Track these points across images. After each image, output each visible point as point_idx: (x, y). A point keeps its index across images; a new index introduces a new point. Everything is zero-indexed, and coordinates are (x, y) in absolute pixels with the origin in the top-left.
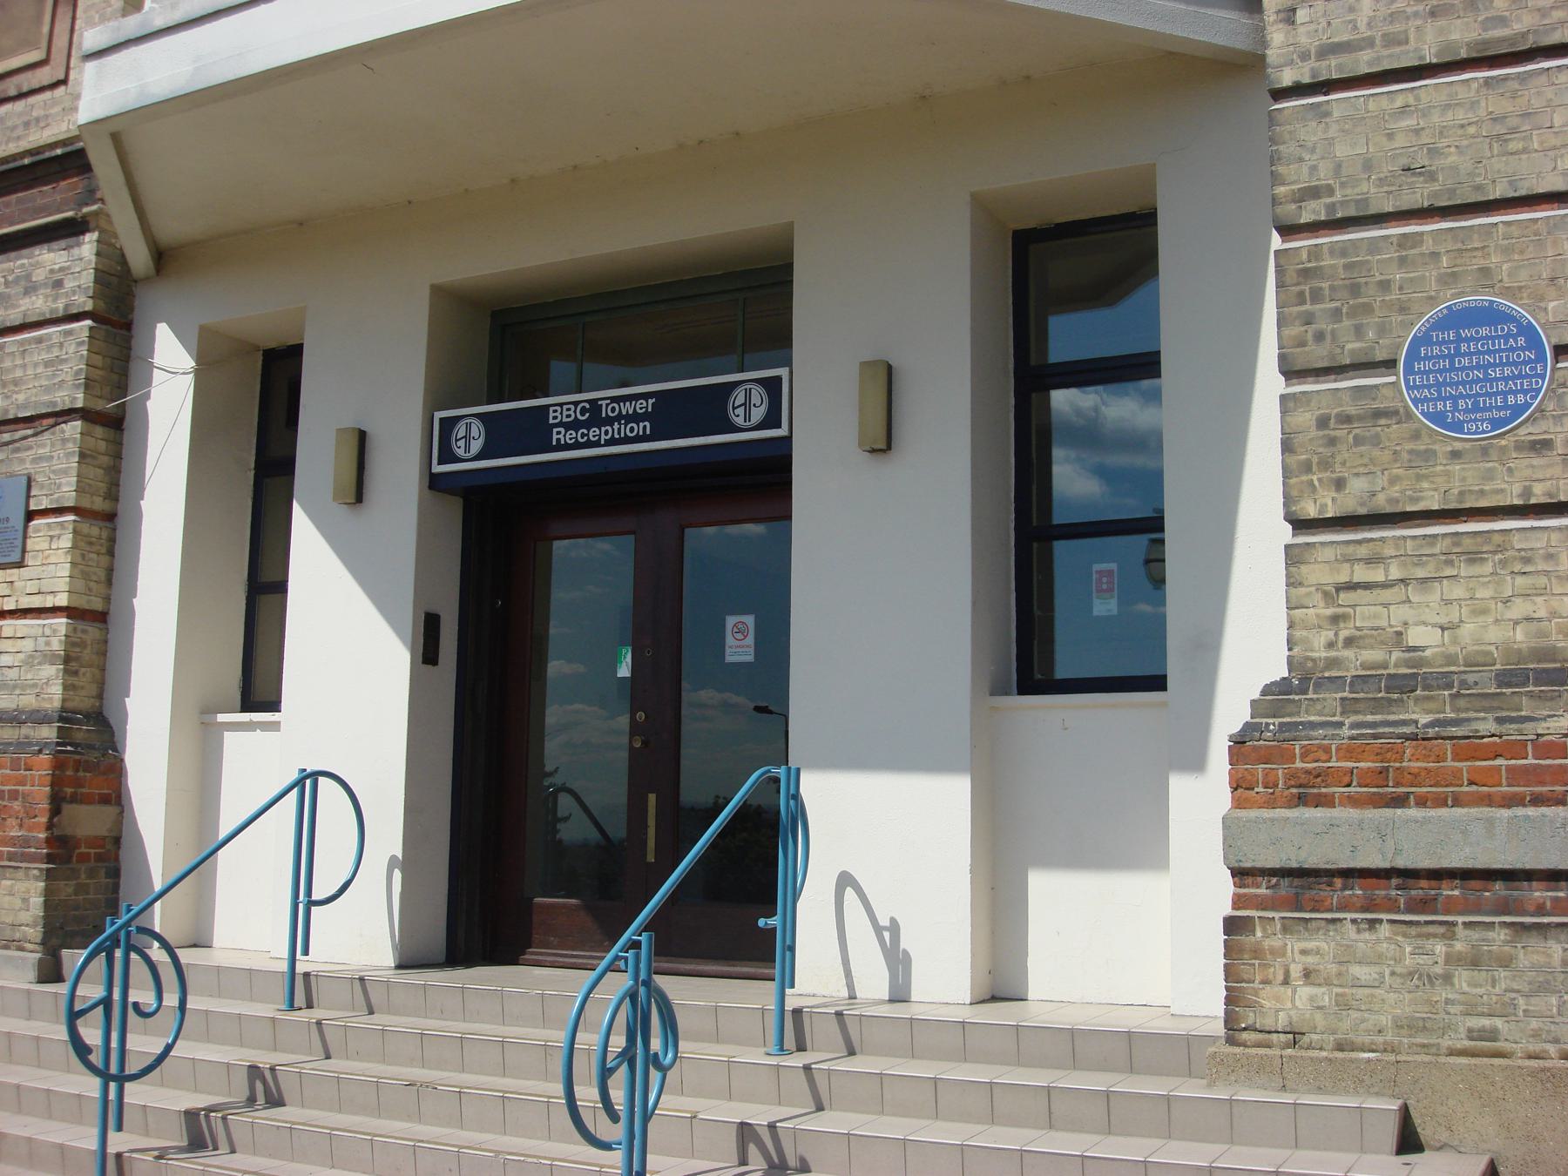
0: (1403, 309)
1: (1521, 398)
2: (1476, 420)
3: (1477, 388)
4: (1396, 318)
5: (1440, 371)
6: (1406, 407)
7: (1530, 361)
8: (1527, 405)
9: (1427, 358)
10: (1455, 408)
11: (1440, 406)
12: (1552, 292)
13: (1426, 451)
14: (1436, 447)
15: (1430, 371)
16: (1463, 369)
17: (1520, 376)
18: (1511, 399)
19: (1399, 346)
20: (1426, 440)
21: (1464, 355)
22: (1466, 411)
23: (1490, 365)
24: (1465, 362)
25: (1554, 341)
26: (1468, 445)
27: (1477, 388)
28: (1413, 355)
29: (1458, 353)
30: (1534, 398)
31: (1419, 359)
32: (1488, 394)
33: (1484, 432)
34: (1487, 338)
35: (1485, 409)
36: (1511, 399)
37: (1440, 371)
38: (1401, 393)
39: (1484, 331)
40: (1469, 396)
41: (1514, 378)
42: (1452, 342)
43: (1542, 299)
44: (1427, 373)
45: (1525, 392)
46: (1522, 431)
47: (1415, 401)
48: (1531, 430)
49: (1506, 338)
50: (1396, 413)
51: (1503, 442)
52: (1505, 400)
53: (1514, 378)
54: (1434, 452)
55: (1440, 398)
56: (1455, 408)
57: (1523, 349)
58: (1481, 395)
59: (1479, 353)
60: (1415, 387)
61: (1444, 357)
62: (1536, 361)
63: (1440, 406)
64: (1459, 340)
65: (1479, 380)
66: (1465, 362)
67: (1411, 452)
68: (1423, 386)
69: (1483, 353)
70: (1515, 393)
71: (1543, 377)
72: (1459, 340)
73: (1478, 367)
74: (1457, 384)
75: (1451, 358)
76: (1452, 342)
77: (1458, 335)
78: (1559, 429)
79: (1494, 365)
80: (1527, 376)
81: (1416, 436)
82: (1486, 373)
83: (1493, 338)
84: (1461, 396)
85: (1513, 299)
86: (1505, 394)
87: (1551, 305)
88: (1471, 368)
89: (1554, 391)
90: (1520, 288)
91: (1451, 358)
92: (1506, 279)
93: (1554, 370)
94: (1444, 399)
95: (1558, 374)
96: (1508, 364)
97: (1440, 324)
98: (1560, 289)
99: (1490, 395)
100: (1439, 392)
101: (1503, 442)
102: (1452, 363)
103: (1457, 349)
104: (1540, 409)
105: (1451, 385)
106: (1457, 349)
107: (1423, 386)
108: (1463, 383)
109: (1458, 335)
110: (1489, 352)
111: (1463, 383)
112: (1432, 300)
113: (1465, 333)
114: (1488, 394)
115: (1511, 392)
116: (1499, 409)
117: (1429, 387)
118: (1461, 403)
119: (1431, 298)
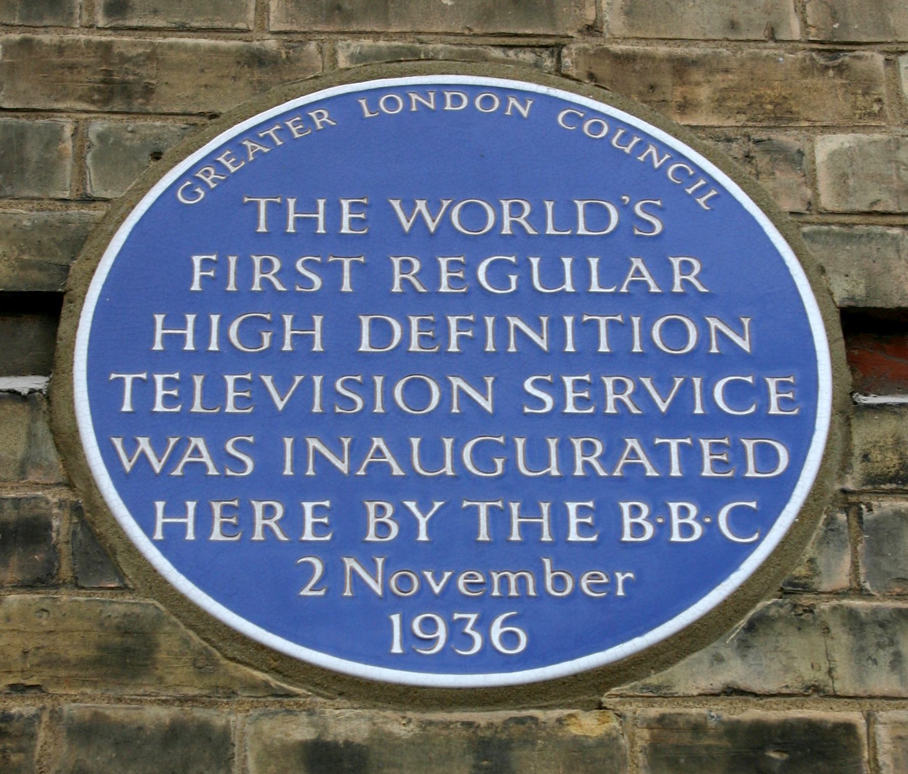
0: (118, 88)
1: (685, 521)
2: (449, 601)
3: (460, 456)
4: (78, 124)
5: (281, 364)
6: (88, 511)
7: (730, 360)
8: (718, 557)
9: (215, 298)
10: (346, 534)
11: (265, 519)
12: (828, 96)
13: (173, 734)
14: (220, 717)
15: (229, 358)
16: (397, 362)
17: (678, 419)
18: (635, 520)
19: (83, 243)
20: (180, 676)
21: (407, 303)
22: (404, 552)
23: (531, 359)
24: (408, 333)
25: (844, 289)
26: (400, 725)
27: (460, 456)
28: (150, 278)
29: (374, 292)
30: (761, 521)
31: (178, 303)
32: (510, 485)
33: (489, 660)
34: (520, 242)
35: (499, 553)
36: (635, 520)
37: (281, 364)
38: (68, 445)
39: (502, 216)
40: (424, 491)
41: (649, 424)
42: (347, 244)
43: (782, 115)
44: (214, 365)
45: (708, 496)
46: (692, 676)
47: (139, 487)
48: (736, 672)
49: (615, 251)
50: (33, 531)
51: (588, 725)
52: (606, 520)
53: (649, 424)
54: (219, 745)
55: (268, 482)
56: (346, 534)
57: (694, 303)
58: (480, 488)
59: (472, 299)
60: (144, 420)
61: (303, 305)
62: (763, 360)
63: (265, 519)
64: (379, 238)
65: (469, 420)
66: (408, 333)
67: (87, 732)
68: (188, 424)
69: (501, 307)
70: (658, 492)
71: (798, 433)
72: (379, 238)
73: (472, 362)
74: (365, 425)
75: (341, 313)
76: (347, 244)
77: (378, 219)
78: (884, 681)
79: (553, 363)
80: (714, 421)
81: (126, 655)
82: (511, 396)
83: (551, 251)
84: (381, 483)
85: (652, 103)
86: (604, 495)
87: (825, 147)
88: (442, 364)
89: (848, 501)
90: (681, 67)
91: (341, 313)
92: (614, 23)
93: (847, 412)
94: (294, 492)
95: (864, 434)
96: (622, 361)
97: (293, 166)
98: (867, 85)
99: (531, 493)
100: (268, 458)
101: (588, 725)
102: (343, 333)
103: (373, 276)
104: (786, 582)
105: (330, 426)
106: (373, 276)
107: (188, 424)
108: (395, 426)
109: (378, 219)
110: (528, 303)
111: (395, 426)
112: (267, 71)
113: (413, 213)
114: (510, 485)
115: (633, 483)
116: (571, 558)
117: (216, 427)
118: (378, 518)
119: (258, 59)
